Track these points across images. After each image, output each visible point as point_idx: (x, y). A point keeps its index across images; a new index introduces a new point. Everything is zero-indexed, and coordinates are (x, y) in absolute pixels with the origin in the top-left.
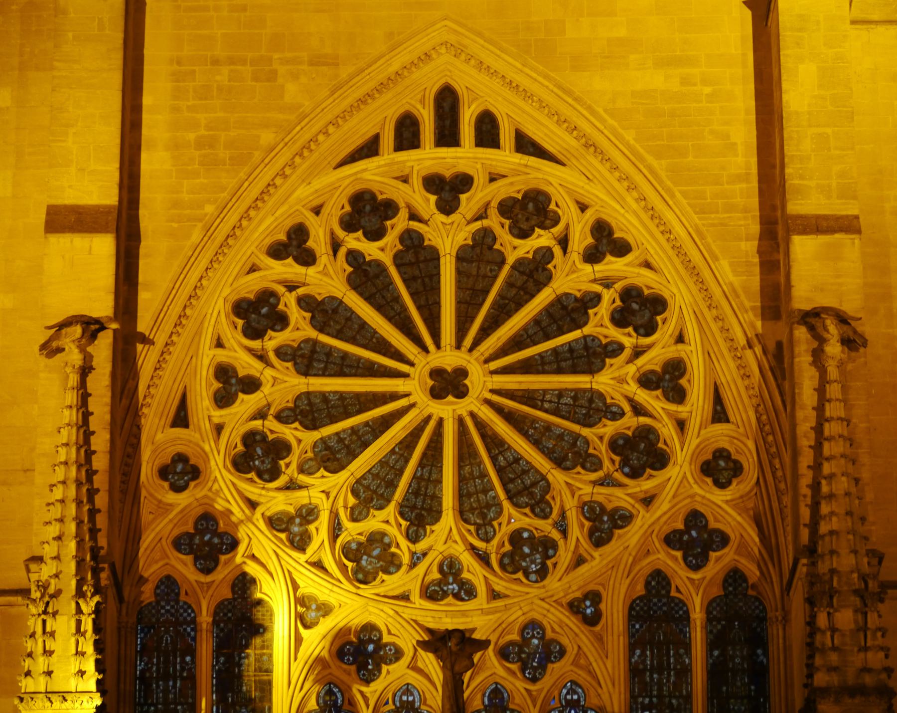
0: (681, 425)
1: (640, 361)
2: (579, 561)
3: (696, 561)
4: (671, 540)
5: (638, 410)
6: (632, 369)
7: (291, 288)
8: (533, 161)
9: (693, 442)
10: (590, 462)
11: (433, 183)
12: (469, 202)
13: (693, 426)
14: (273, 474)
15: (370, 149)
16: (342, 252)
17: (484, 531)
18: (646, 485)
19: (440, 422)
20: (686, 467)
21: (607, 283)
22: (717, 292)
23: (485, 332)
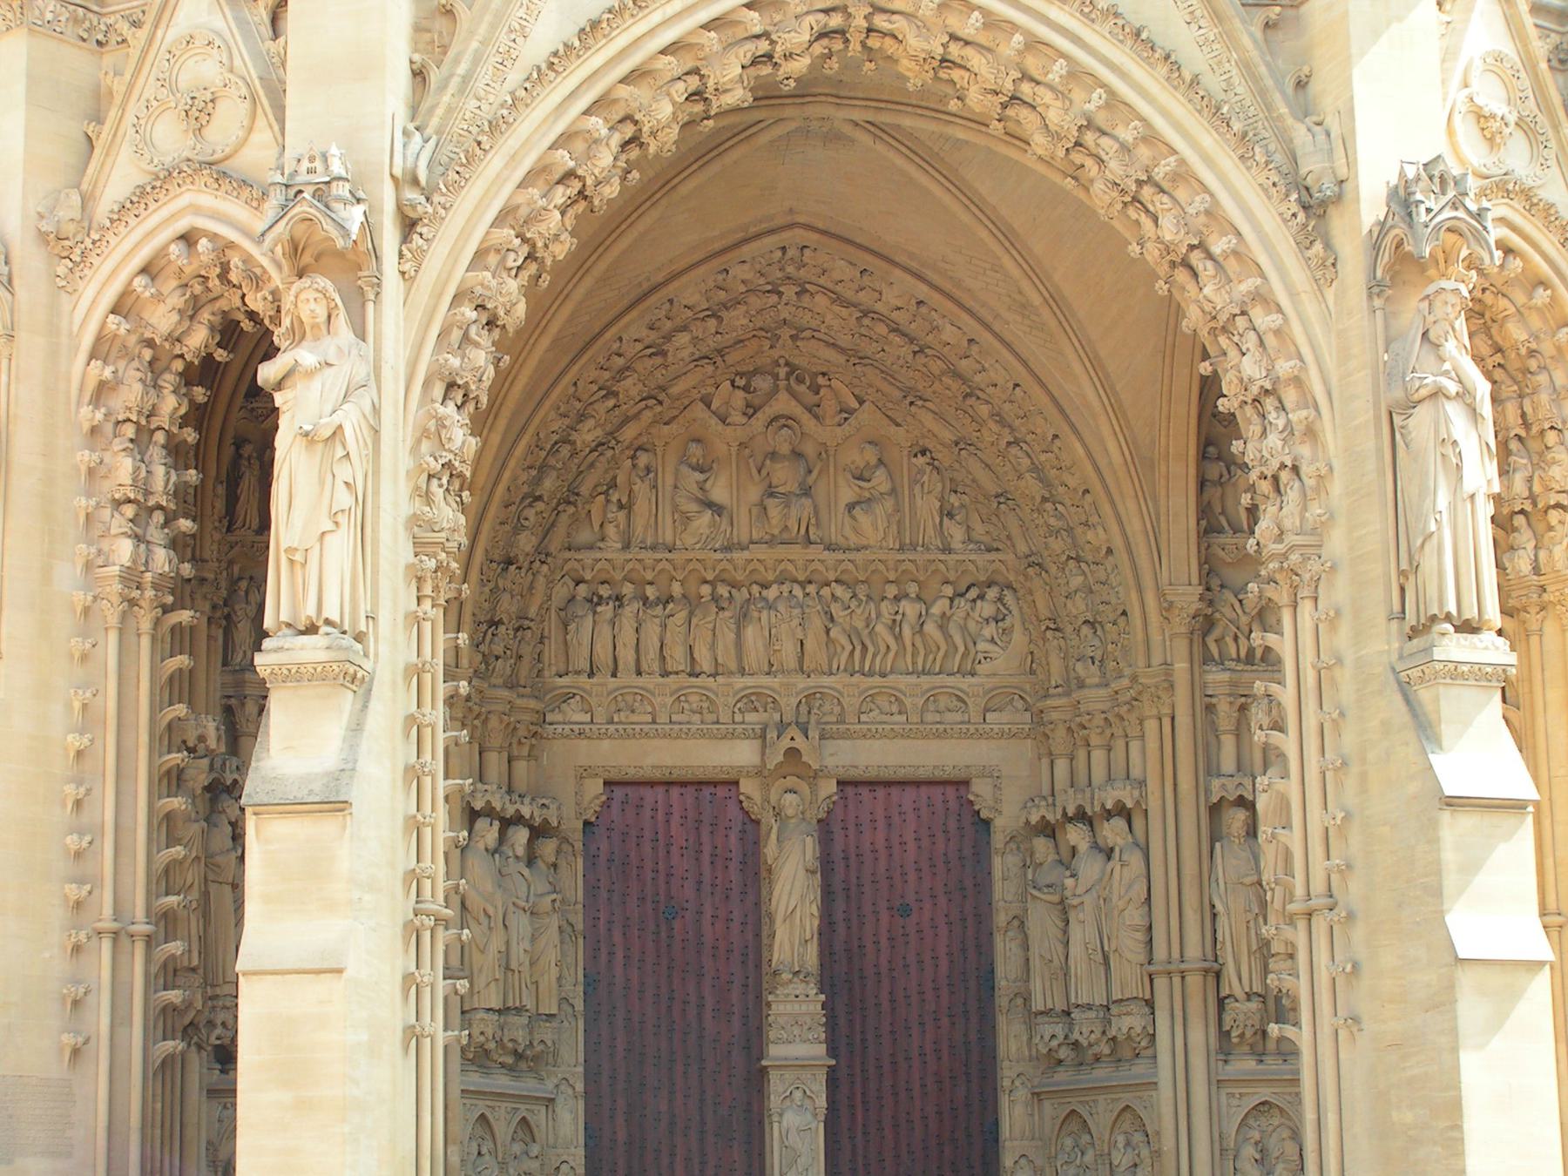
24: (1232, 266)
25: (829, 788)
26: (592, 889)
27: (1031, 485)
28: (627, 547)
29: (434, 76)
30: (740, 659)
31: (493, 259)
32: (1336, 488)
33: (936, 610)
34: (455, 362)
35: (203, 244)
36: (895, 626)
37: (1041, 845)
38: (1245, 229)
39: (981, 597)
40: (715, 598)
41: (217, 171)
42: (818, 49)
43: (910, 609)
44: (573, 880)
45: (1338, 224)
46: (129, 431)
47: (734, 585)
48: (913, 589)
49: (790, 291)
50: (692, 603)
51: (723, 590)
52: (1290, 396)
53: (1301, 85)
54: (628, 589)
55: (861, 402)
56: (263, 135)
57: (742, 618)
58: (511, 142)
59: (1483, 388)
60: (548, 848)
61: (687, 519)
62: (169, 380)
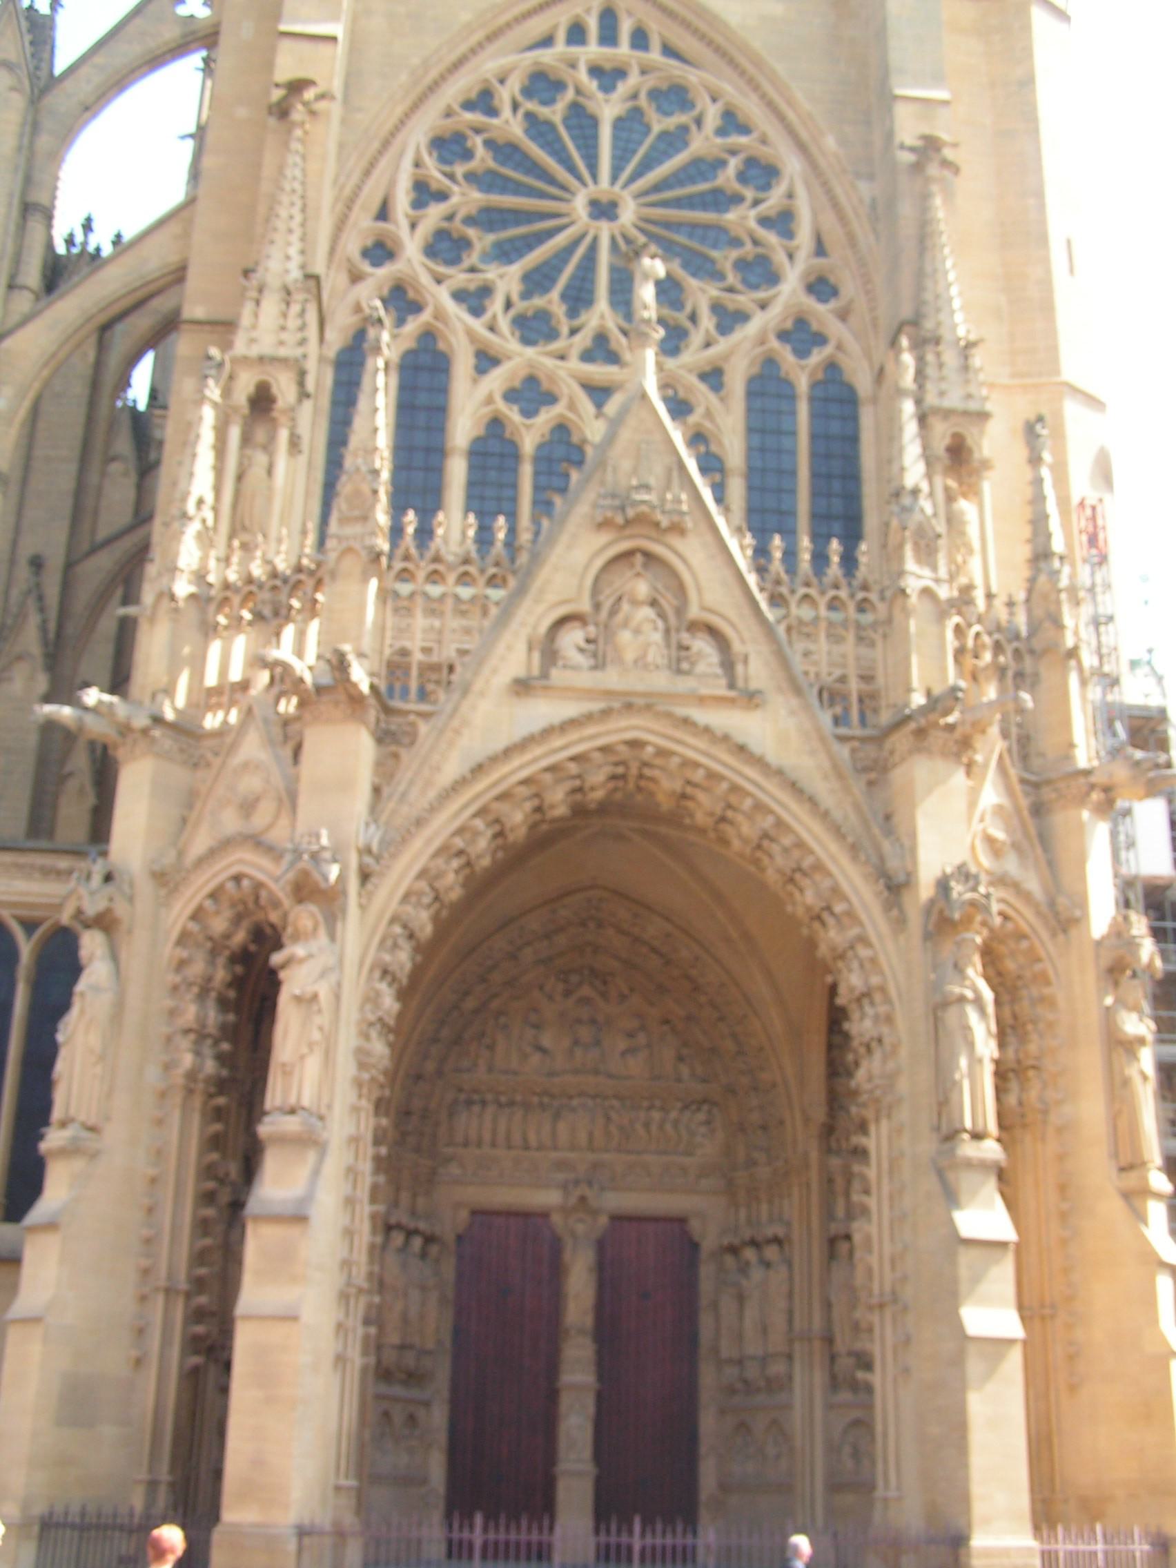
0: (791, 256)
1: (762, 208)
2: (708, 345)
3: (802, 353)
4: (783, 336)
5: (756, 242)
7: (478, 131)
8: (673, 62)
10: (718, 276)
11: (595, 71)
12: (623, 88)
15: (547, 41)
16: (521, 112)
18: (761, 295)
19: (595, 240)
21: (733, 152)
24: (846, 921)
25: (603, 1220)
26: (460, 1276)
27: (729, 1045)
29: (386, 791)
31: (413, 899)
32: (904, 1052)
34: (387, 958)
35: (246, 883)
36: (647, 1125)
37: (729, 1260)
38: (854, 899)
39: (699, 1109)
41: (256, 842)
43: (656, 1115)
44: (449, 1269)
45: (907, 898)
46: (196, 990)
47: (552, 1096)
48: (658, 1103)
49: (592, 925)
50: (527, 1106)
52: (878, 997)
53: (888, 817)
54: (489, 1097)
56: (284, 821)
57: (557, 1116)
58: (427, 832)
59: (988, 995)
60: (434, 1249)
62: (221, 960)
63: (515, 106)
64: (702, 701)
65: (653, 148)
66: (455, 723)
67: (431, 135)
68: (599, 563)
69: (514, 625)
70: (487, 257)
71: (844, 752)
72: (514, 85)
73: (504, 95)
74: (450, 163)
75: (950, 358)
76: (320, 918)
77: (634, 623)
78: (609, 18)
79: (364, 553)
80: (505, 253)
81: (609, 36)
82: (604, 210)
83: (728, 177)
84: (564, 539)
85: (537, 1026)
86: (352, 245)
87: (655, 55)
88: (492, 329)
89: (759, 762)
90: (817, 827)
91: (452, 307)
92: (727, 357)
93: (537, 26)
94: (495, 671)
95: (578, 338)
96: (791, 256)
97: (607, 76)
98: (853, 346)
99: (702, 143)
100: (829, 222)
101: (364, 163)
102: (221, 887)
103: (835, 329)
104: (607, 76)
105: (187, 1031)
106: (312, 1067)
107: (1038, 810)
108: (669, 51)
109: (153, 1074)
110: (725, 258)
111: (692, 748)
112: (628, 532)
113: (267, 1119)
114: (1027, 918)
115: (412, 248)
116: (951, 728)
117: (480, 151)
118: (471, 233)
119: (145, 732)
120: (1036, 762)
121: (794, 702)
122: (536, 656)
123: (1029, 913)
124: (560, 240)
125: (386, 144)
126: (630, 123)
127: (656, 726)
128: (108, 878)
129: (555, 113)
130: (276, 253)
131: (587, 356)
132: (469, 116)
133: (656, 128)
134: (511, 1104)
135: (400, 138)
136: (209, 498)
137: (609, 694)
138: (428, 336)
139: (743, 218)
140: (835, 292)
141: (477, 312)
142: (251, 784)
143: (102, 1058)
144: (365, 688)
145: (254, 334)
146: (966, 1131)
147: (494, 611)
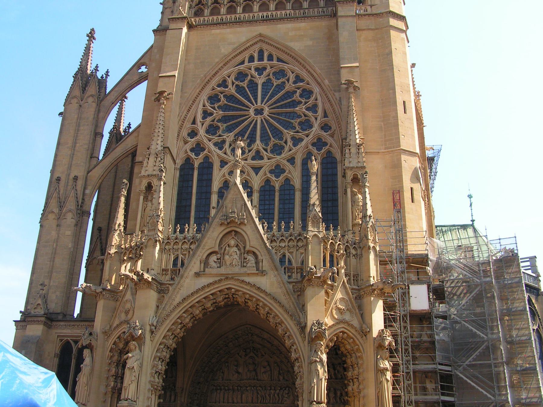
0: (316, 119)
2: (290, 150)
4: (313, 144)
5: (305, 116)
6: (304, 106)
9: (318, 121)
11: (257, 69)
13: (319, 118)
14: (216, 133)
15: (243, 63)
16: (235, 85)
17: (267, 145)
19: (257, 120)
20: (317, 127)
22: (324, 87)
23: (268, 101)
28: (223, 380)
29: (160, 307)
30: (242, 400)
31: (168, 337)
33: (277, 392)
34: (159, 354)
36: (269, 395)
38: (291, 331)
40: (238, 389)
42: (225, 301)
43: (272, 392)
46: (115, 364)
47: (241, 387)
50: (233, 390)
51: (239, 388)
54: (223, 387)
55: (265, 353)
58: (171, 318)
61: (233, 375)
63: (233, 83)
64: (249, 275)
65: (274, 90)
66: (179, 287)
67: (208, 96)
68: (221, 236)
69: (196, 257)
70: (224, 131)
71: (291, 286)
72: (233, 77)
73: (229, 81)
74: (214, 104)
75: (353, 150)
76: (137, 345)
77: (230, 253)
78: (261, 53)
79: (153, 240)
80: (229, 129)
81: (261, 59)
82: (259, 112)
83: (297, 96)
84: (211, 229)
85: (237, 366)
86: (185, 133)
87: (275, 62)
88: (225, 153)
89: (264, 292)
90: (281, 310)
91: (213, 148)
92: (295, 154)
93: (239, 59)
94: (191, 270)
95: (250, 153)
96: (316, 119)
97: (260, 70)
98: (335, 144)
99: (290, 86)
100: (328, 106)
101: (188, 108)
102: (120, 335)
103: (329, 140)
104: (260, 70)
105: (113, 375)
106: (133, 387)
107: (359, 298)
108: (279, 60)
109: (103, 389)
110: (295, 122)
111: (246, 289)
112: (229, 226)
113: (120, 402)
114: (351, 332)
115: (202, 131)
116: (319, 277)
117: (222, 99)
118: (219, 124)
119: (101, 292)
120: (360, 282)
121: (276, 273)
122: (202, 265)
123: (353, 331)
124: (246, 123)
125: (194, 101)
126: (267, 84)
127: (235, 283)
128: (91, 334)
129: (245, 84)
130: (154, 143)
131: (253, 159)
132: (219, 89)
133: (275, 84)
134: (229, 390)
135: (198, 98)
136: (122, 223)
137: (222, 274)
138: (207, 158)
139: (301, 109)
140: (330, 128)
141: (221, 149)
142: (128, 306)
143: (87, 384)
144: (150, 280)
145: (147, 168)
146: (315, 401)
147: (191, 252)
